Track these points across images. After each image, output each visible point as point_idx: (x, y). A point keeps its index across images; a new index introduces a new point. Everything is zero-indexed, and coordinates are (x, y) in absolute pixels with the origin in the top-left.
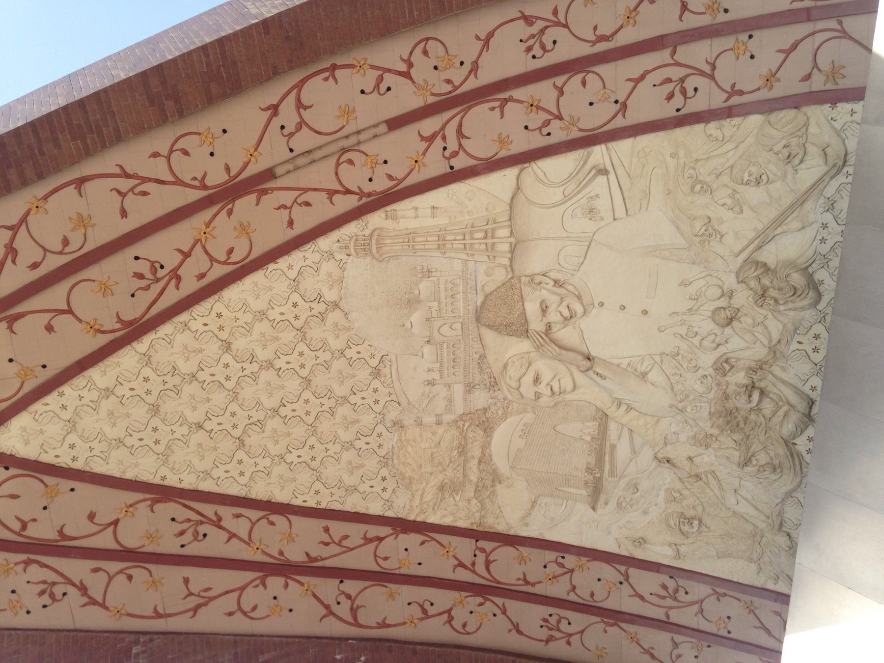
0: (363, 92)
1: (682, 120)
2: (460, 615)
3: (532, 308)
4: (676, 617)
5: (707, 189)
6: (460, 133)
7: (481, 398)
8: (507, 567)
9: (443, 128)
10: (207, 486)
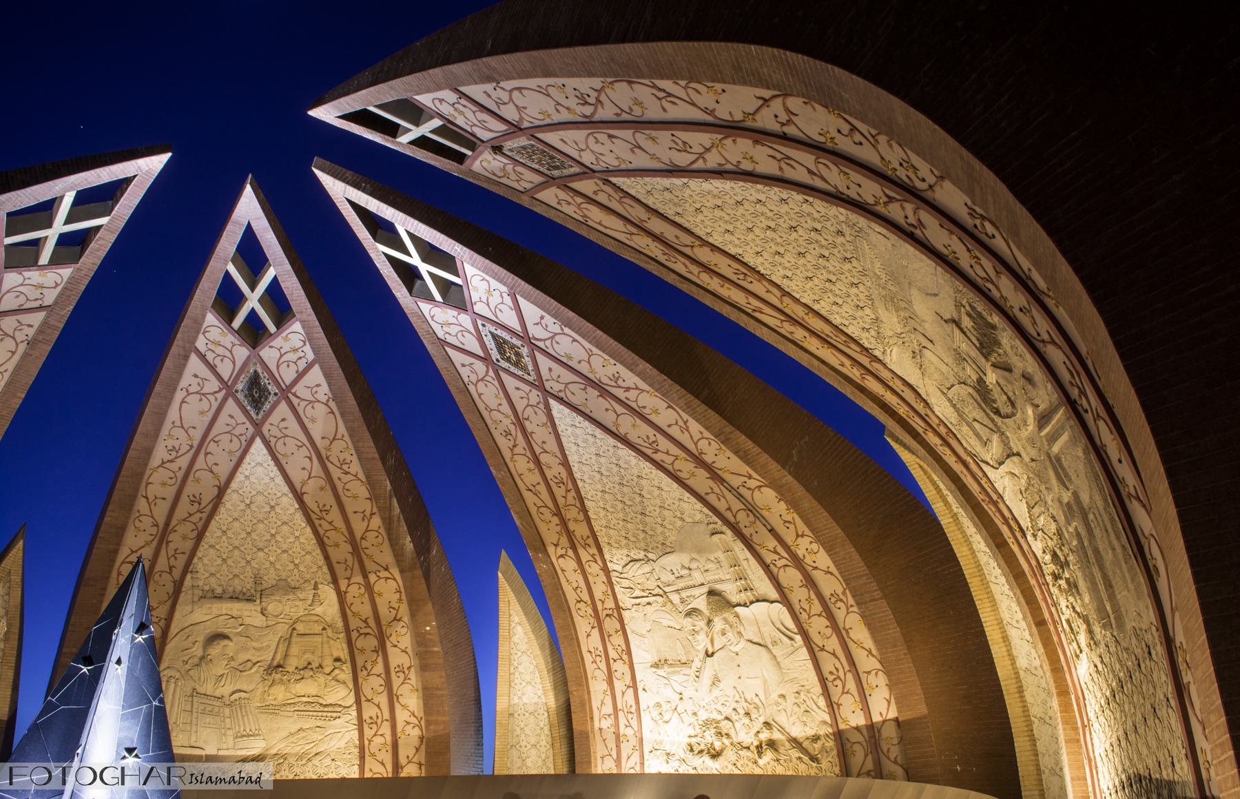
1: (823, 681)
2: (581, 605)
4: (621, 714)
8: (611, 625)
10: (580, 484)
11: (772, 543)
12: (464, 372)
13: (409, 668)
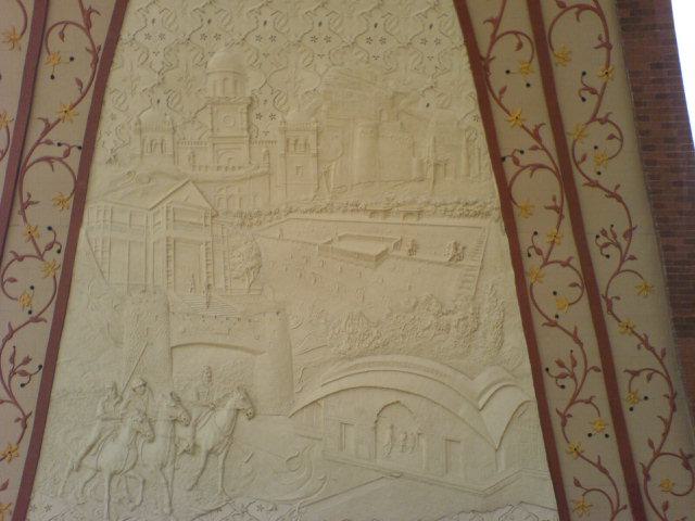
0: (584, 74)
9: (544, 149)
11: (538, 115)
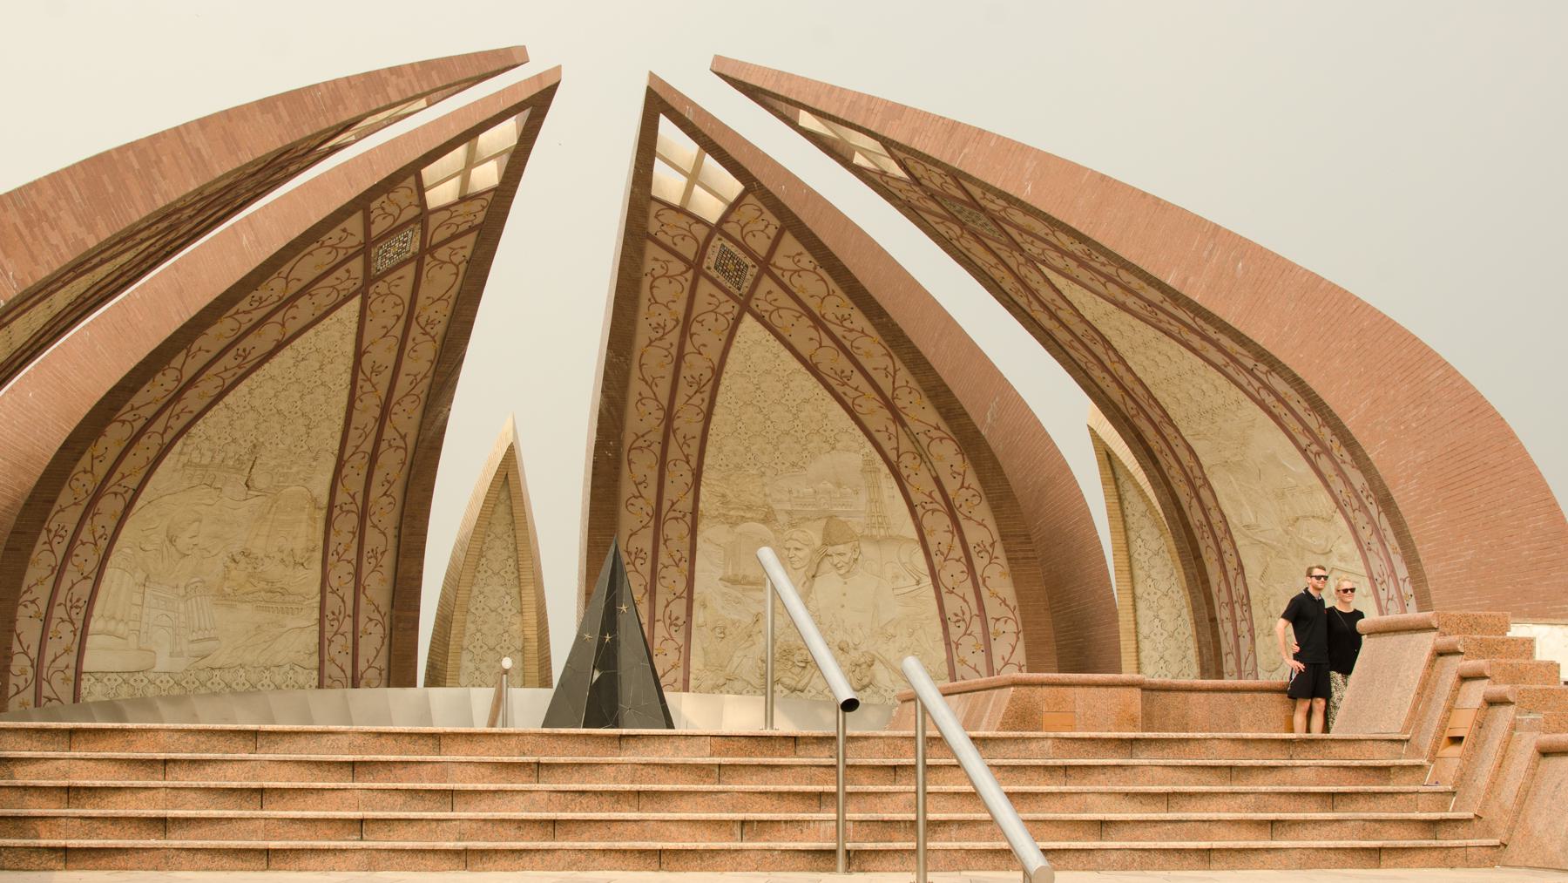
1: (944, 622)
2: (640, 502)
3: (841, 548)
5: (911, 635)
6: (934, 511)
7: (783, 518)
8: (675, 531)
10: (722, 389)
12: (649, 265)
13: (383, 553)
